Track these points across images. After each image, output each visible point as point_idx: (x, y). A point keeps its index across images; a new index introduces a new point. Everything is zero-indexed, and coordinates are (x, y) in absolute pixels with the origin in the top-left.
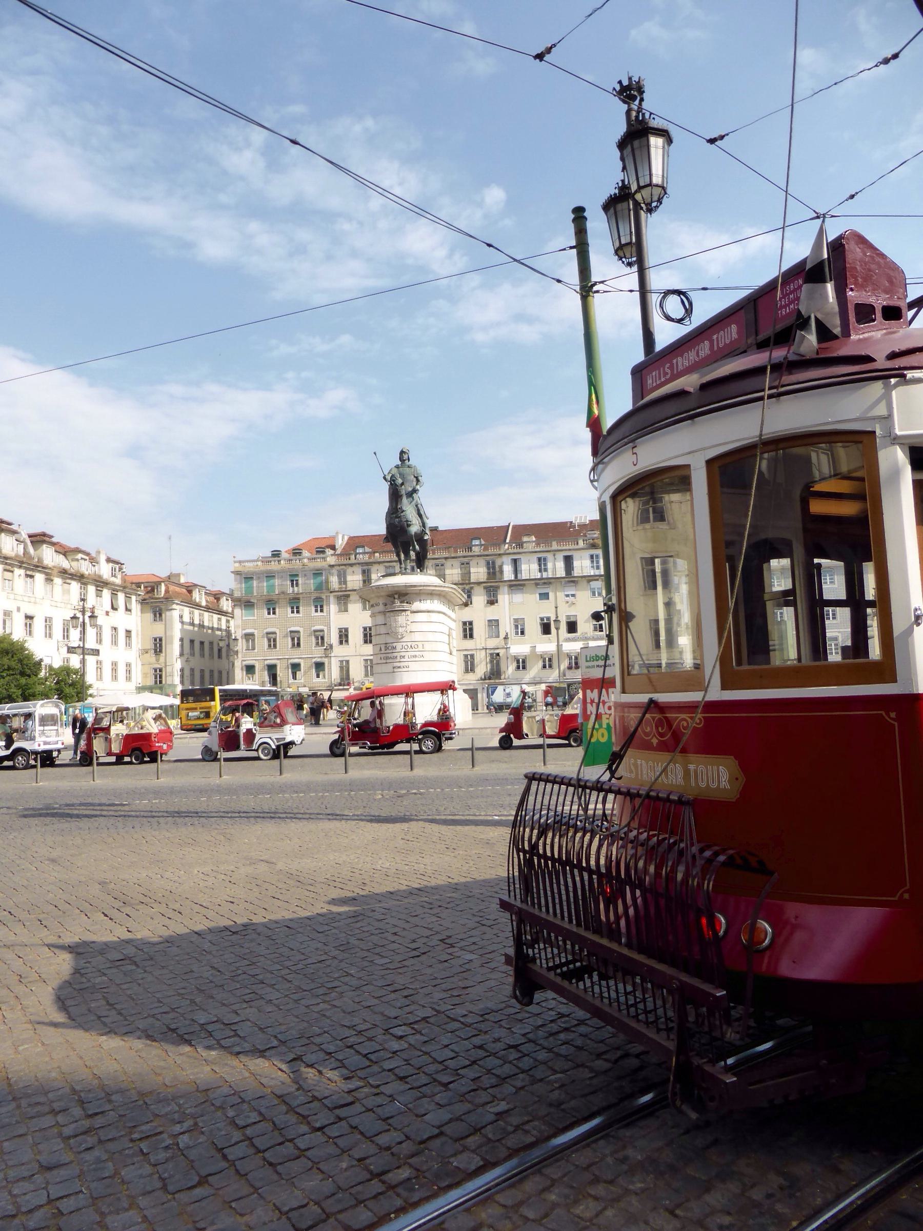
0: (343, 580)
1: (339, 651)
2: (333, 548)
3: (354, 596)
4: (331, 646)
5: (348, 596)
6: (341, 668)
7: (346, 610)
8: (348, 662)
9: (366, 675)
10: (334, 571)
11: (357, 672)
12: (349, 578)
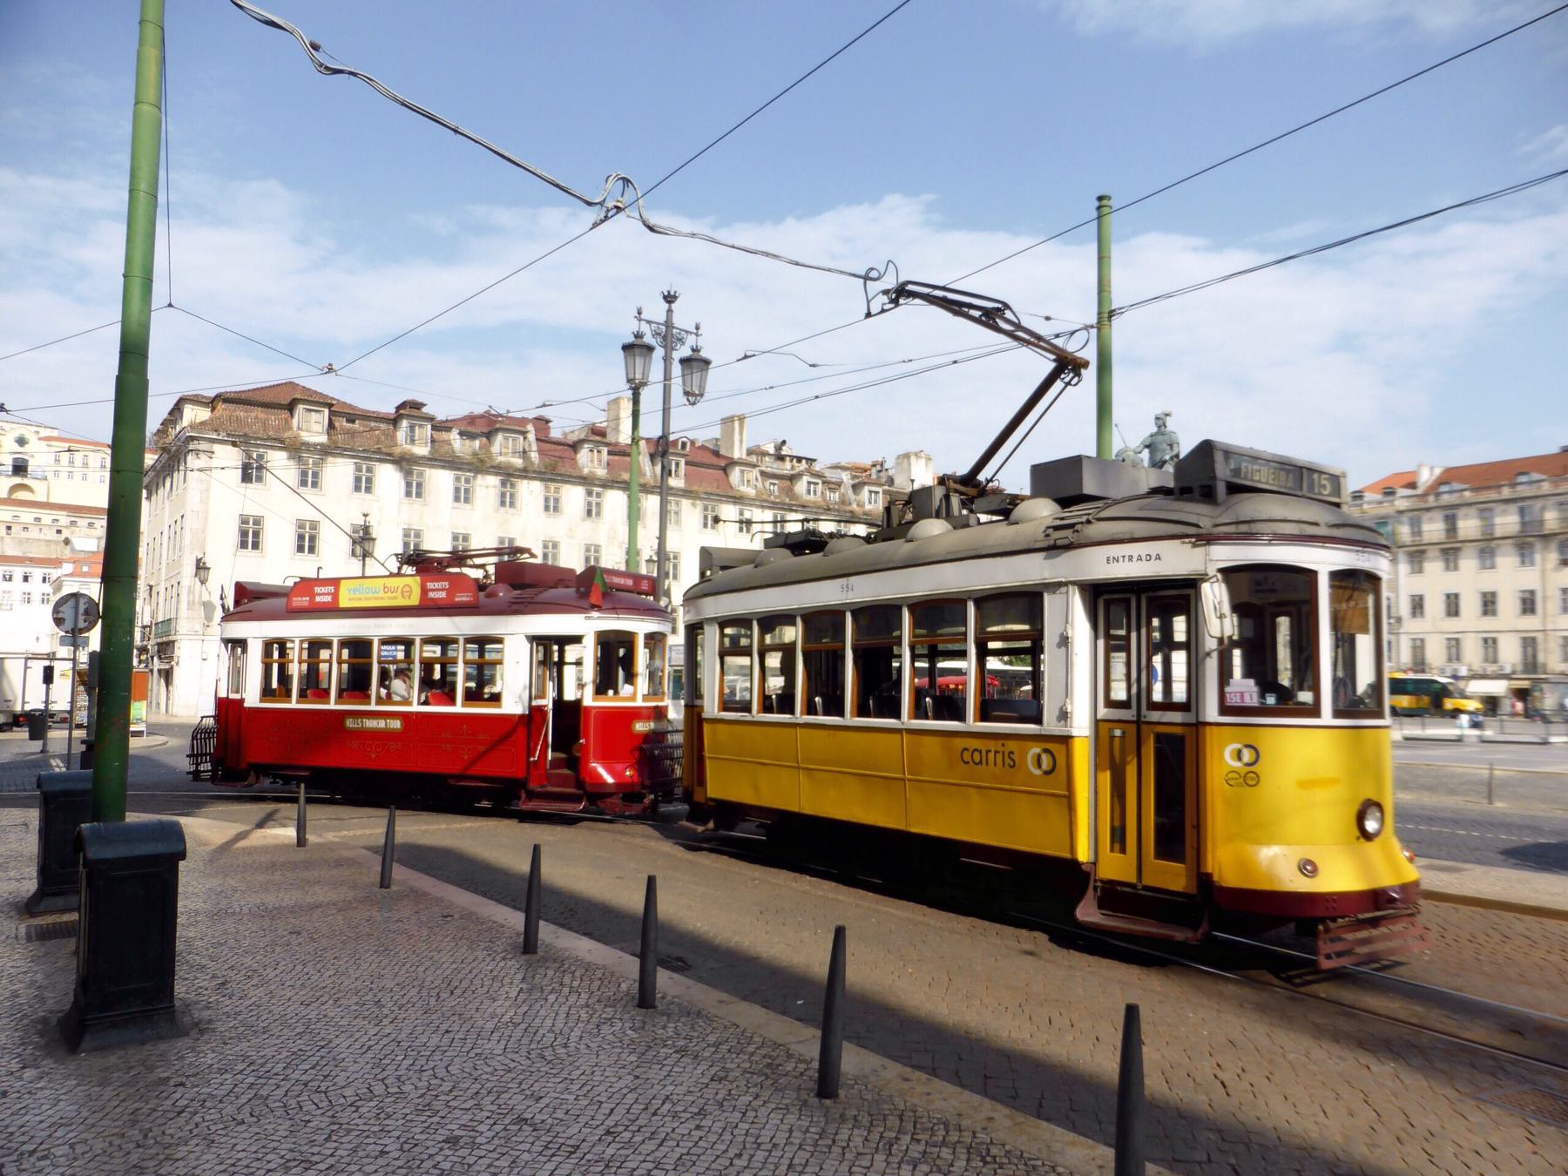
0: (1417, 532)
1: (1411, 626)
2: (1412, 485)
3: (1433, 552)
4: (1399, 620)
5: (1423, 552)
6: (1414, 648)
7: (1421, 571)
8: (1422, 640)
9: (1450, 660)
10: (1405, 518)
11: (1435, 654)
12: (1426, 527)
